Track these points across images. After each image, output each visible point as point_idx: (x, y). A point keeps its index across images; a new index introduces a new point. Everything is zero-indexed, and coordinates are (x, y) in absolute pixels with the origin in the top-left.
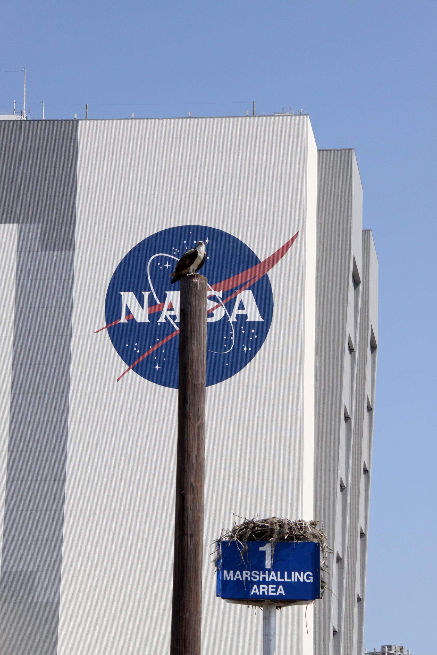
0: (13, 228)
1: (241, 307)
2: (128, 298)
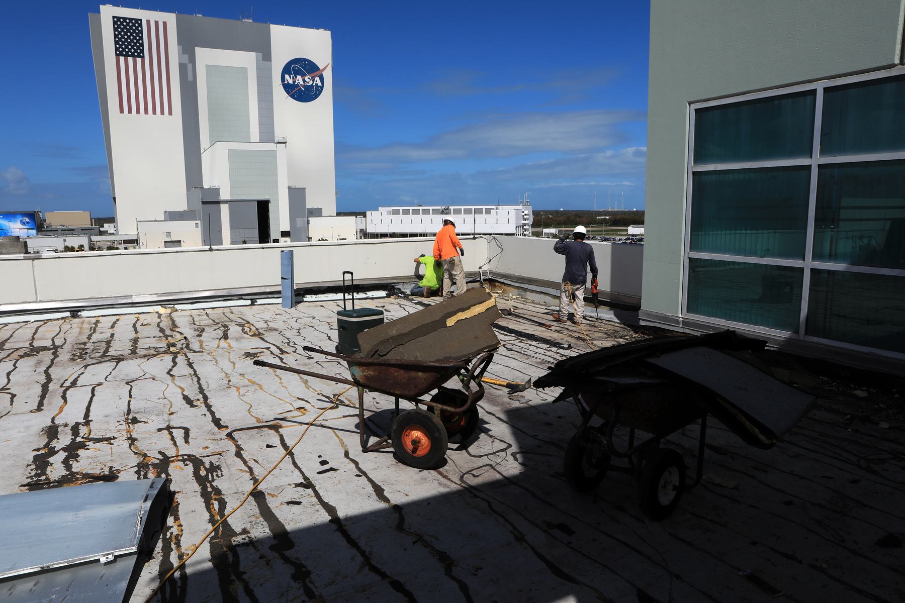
0: (254, 54)
2: (287, 76)
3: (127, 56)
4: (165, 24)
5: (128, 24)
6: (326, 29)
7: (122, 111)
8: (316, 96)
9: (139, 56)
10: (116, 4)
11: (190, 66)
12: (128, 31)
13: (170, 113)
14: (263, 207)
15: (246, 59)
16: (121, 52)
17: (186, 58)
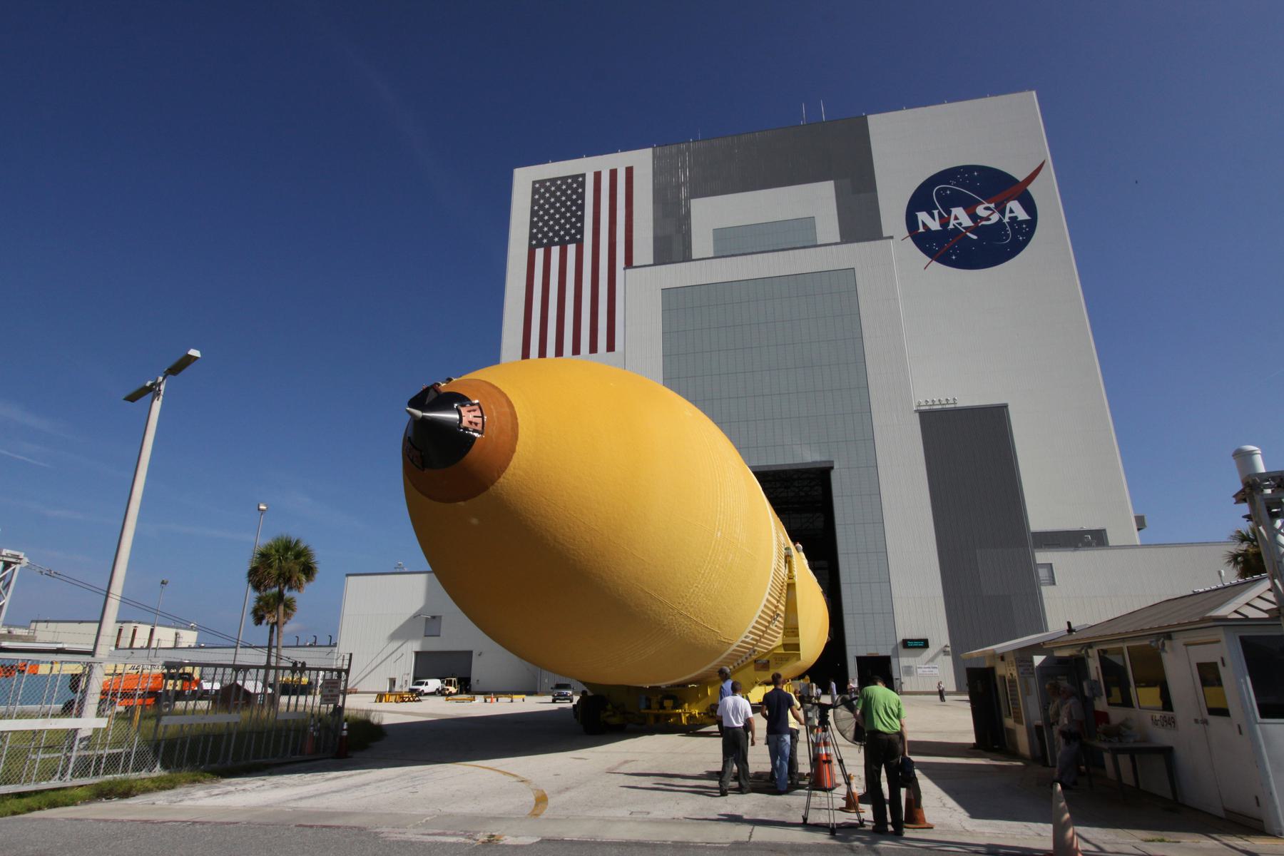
0: (832, 183)
1: (1011, 211)
3: (551, 243)
4: (629, 171)
7: (526, 355)
12: (558, 199)
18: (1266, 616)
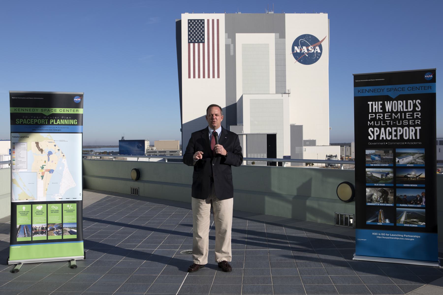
2: (296, 48)
3: (195, 42)
5: (196, 23)
6: (324, 13)
7: (189, 77)
8: (316, 60)
9: (201, 42)
10: (190, 12)
11: (232, 46)
13: (218, 77)
14: (272, 140)
15: (269, 38)
16: (191, 41)
17: (230, 40)
18: (324, 165)
